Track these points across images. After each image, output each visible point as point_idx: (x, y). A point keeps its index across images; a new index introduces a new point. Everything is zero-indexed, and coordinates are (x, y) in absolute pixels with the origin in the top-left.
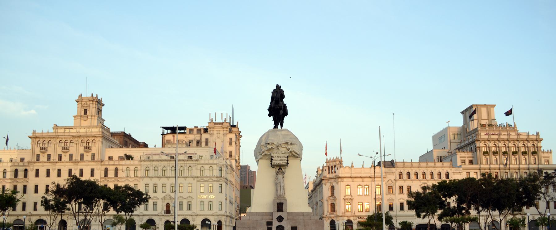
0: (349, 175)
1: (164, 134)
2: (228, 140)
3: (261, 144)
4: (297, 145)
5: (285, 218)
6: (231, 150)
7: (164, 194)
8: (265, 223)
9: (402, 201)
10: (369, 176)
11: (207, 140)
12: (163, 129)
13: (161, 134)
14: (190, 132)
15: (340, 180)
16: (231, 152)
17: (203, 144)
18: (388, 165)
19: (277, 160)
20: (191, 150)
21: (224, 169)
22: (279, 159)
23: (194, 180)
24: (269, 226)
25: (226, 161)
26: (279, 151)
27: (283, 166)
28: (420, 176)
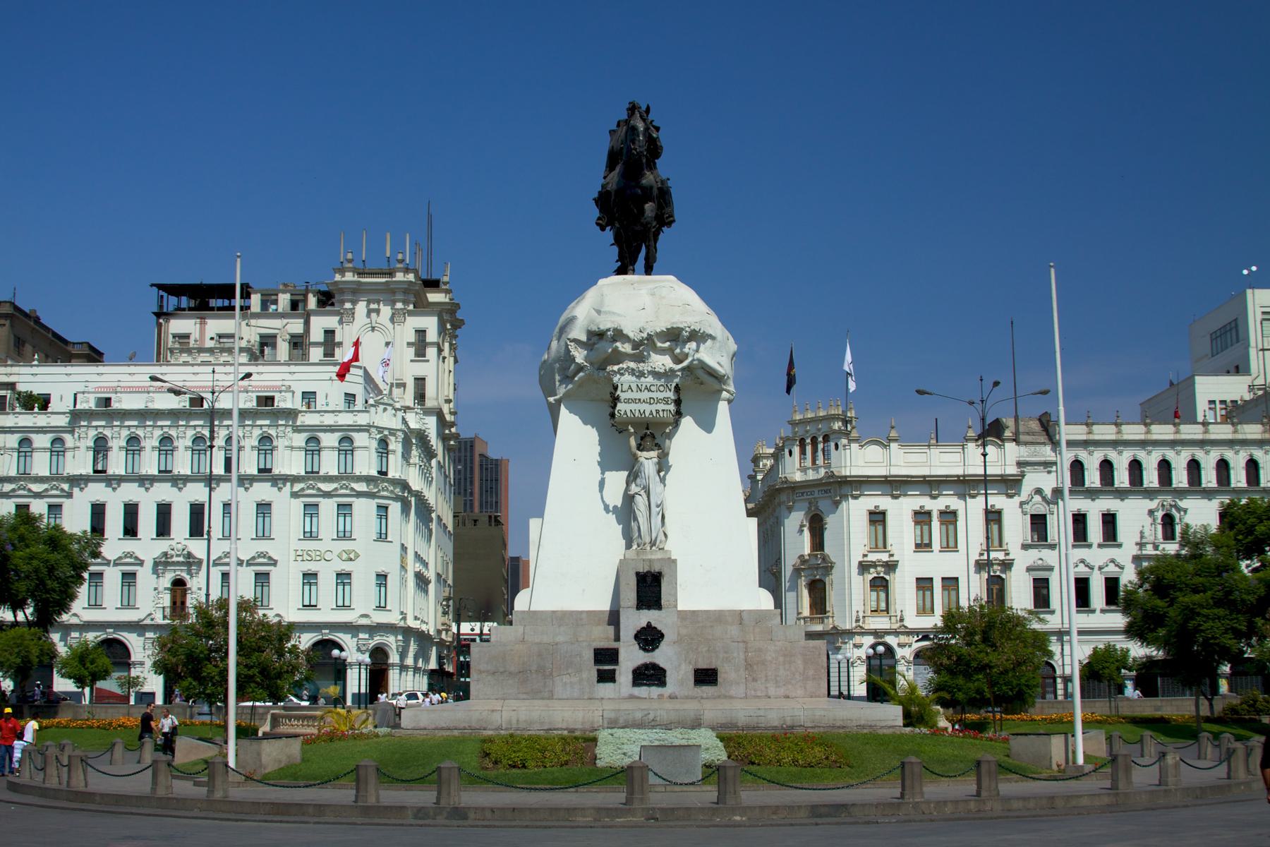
0: (882, 472)
1: (165, 310)
2: (412, 339)
3: (571, 336)
4: (713, 338)
5: (669, 635)
6: (420, 374)
7: (163, 546)
8: (590, 655)
9: (1082, 569)
11: (329, 333)
12: (161, 293)
13: (154, 313)
14: (264, 305)
15: (846, 490)
16: (420, 382)
17: (316, 354)
18: (1028, 434)
19: (634, 401)
20: (267, 377)
21: (395, 445)
23: (280, 489)
24: (601, 667)
25: (403, 419)
27: (662, 424)
28: (1151, 478)
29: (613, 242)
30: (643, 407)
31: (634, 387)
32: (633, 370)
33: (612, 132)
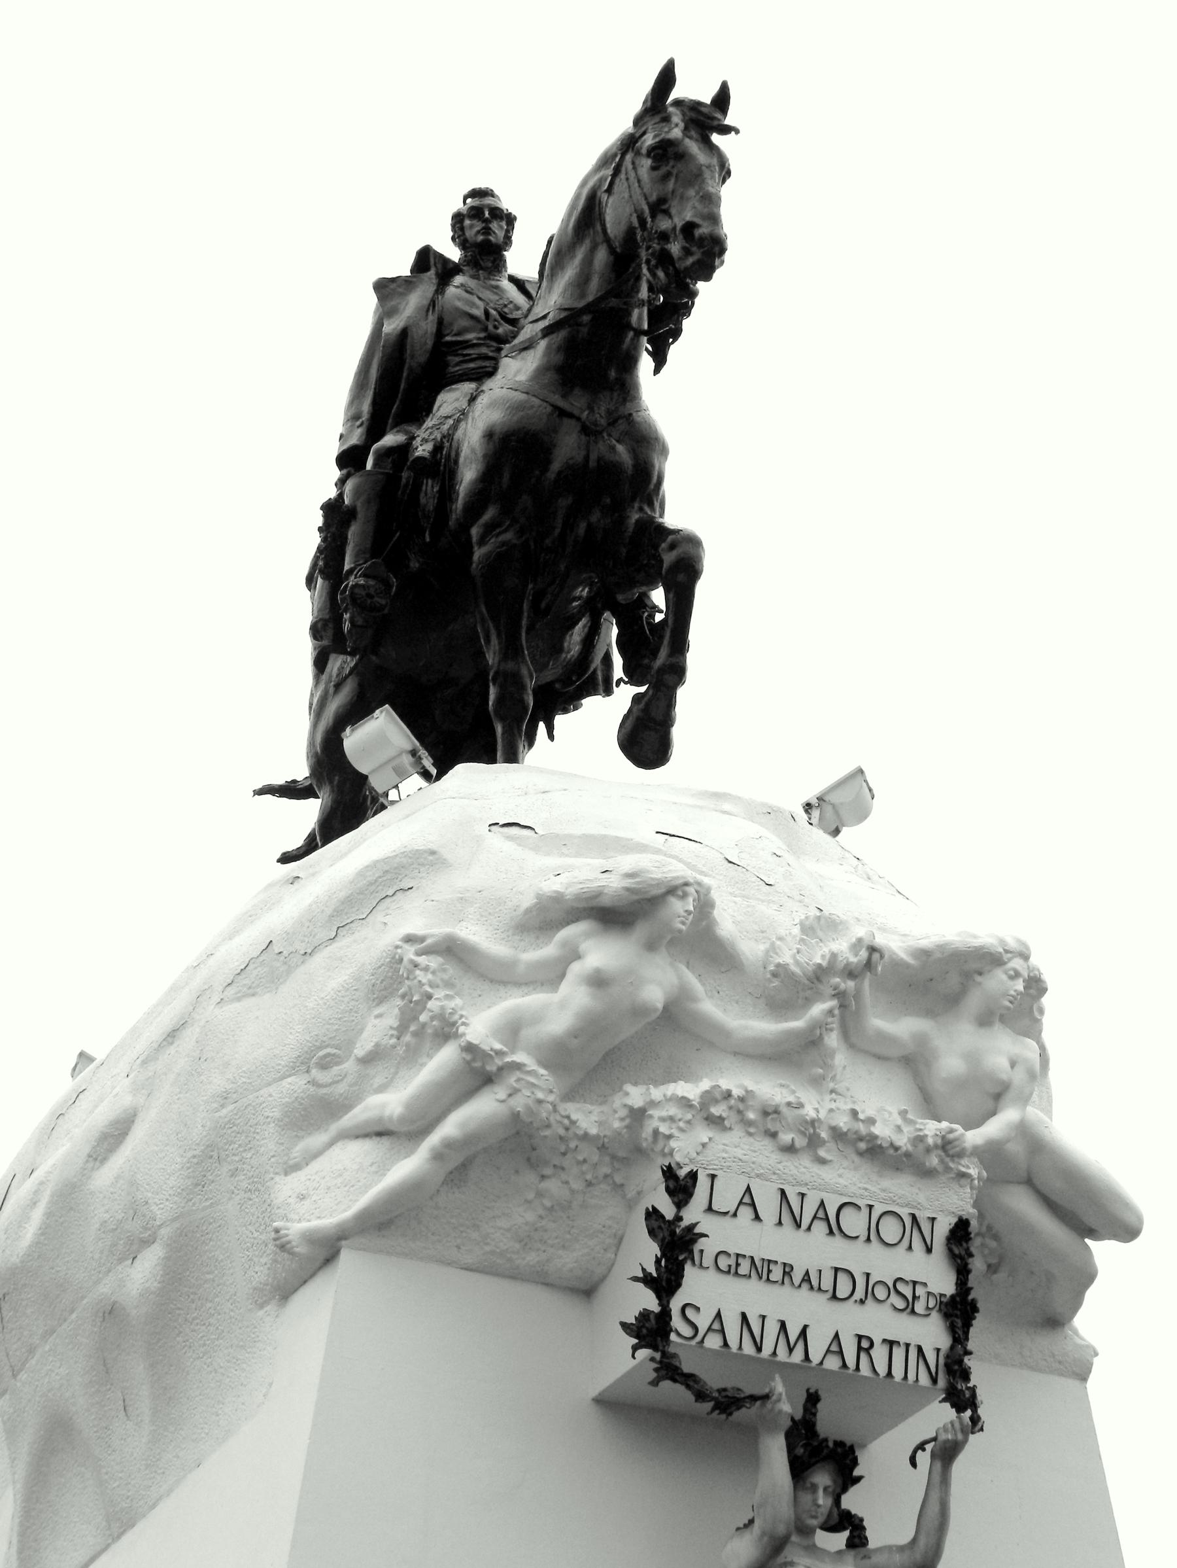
19: (761, 1269)
29: (301, 771)
31: (768, 1204)
32: (769, 1112)
33: (385, 288)
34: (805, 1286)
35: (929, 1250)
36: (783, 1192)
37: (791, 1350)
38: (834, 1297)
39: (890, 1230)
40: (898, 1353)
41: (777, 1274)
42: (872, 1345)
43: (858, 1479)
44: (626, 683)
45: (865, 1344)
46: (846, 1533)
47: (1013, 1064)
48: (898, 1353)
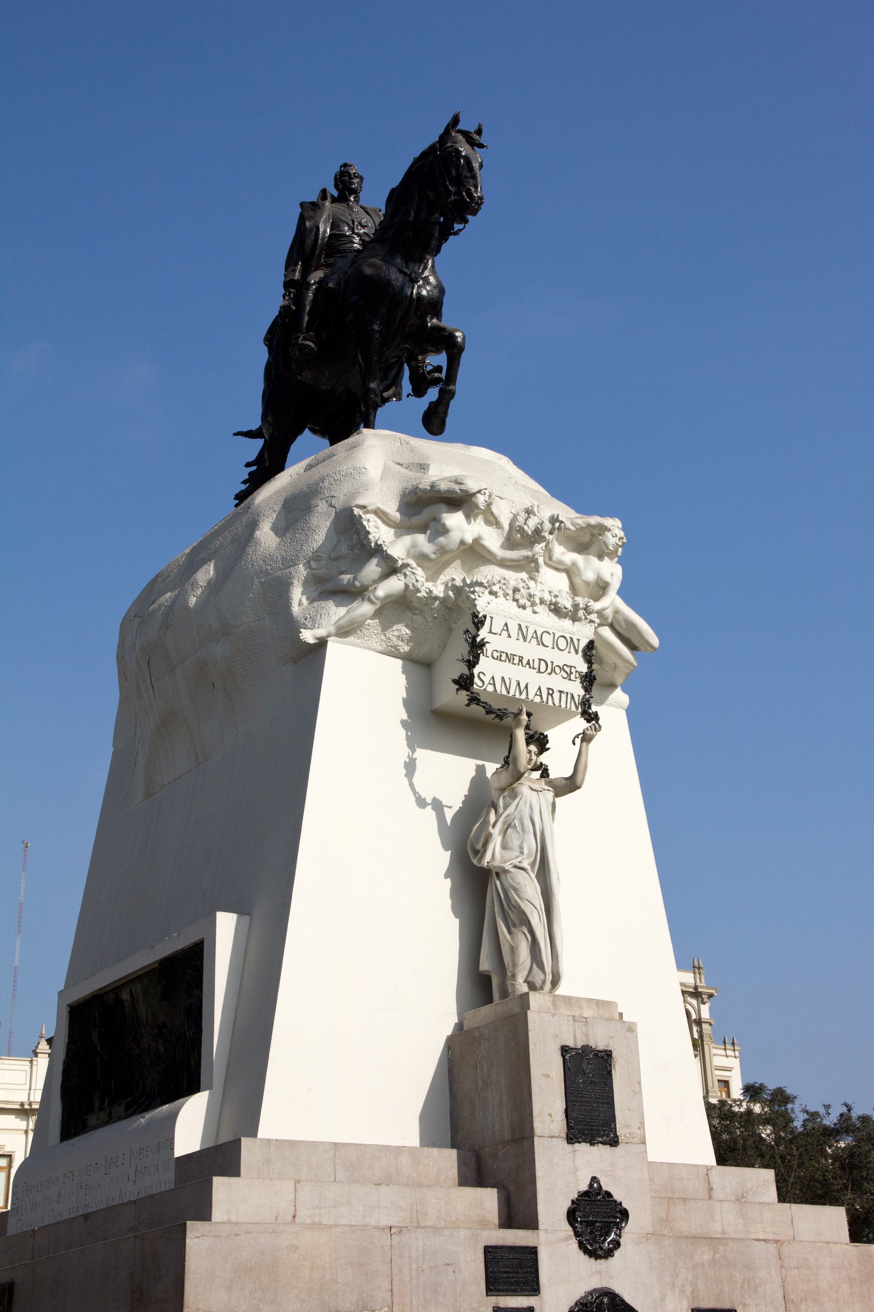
10: (22, 1104)
19: (510, 658)
22: (531, 651)
26: (532, 584)
30: (526, 676)
31: (514, 630)
34: (528, 666)
35: (577, 652)
36: (520, 625)
37: (521, 693)
38: (539, 672)
39: (562, 643)
40: (564, 696)
41: (516, 661)
42: (553, 692)
43: (548, 749)
44: (412, 396)
45: (551, 692)
46: (540, 772)
47: (612, 575)
48: (564, 696)
